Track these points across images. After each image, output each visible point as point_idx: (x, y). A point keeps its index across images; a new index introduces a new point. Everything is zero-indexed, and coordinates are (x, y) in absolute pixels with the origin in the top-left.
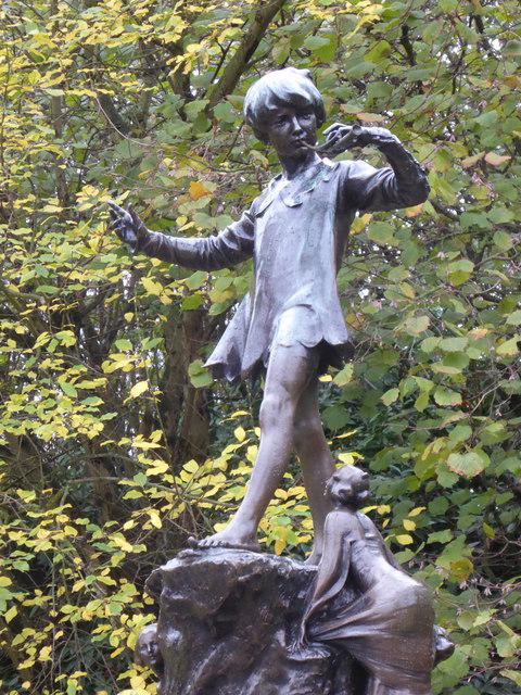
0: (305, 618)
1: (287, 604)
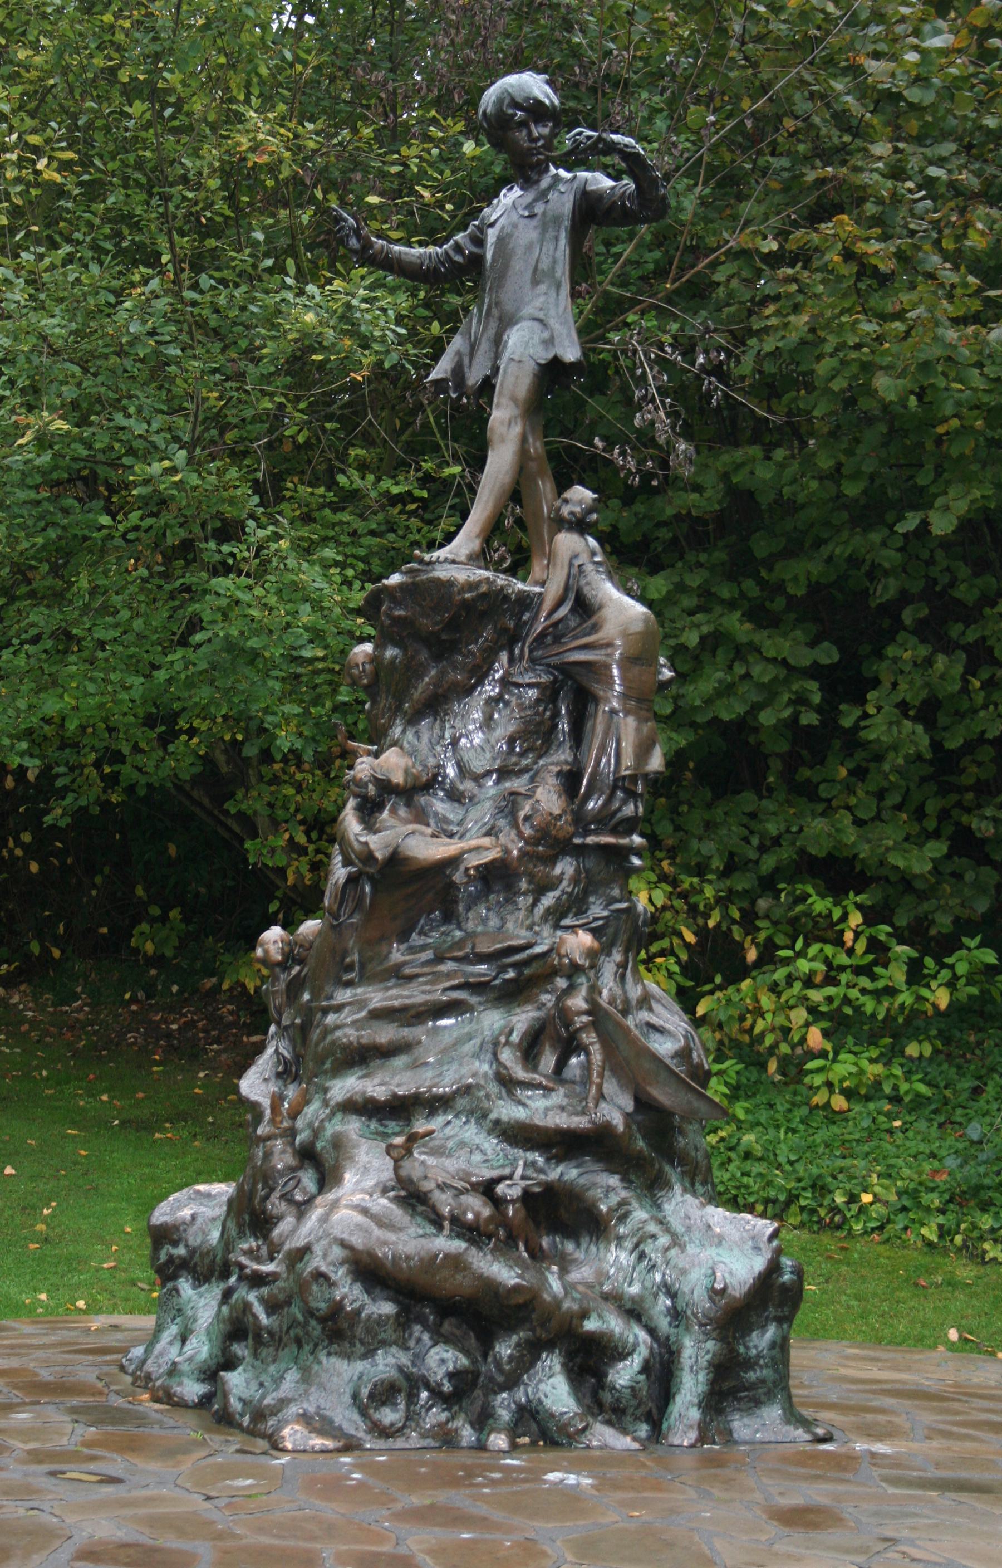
1: (511, 624)
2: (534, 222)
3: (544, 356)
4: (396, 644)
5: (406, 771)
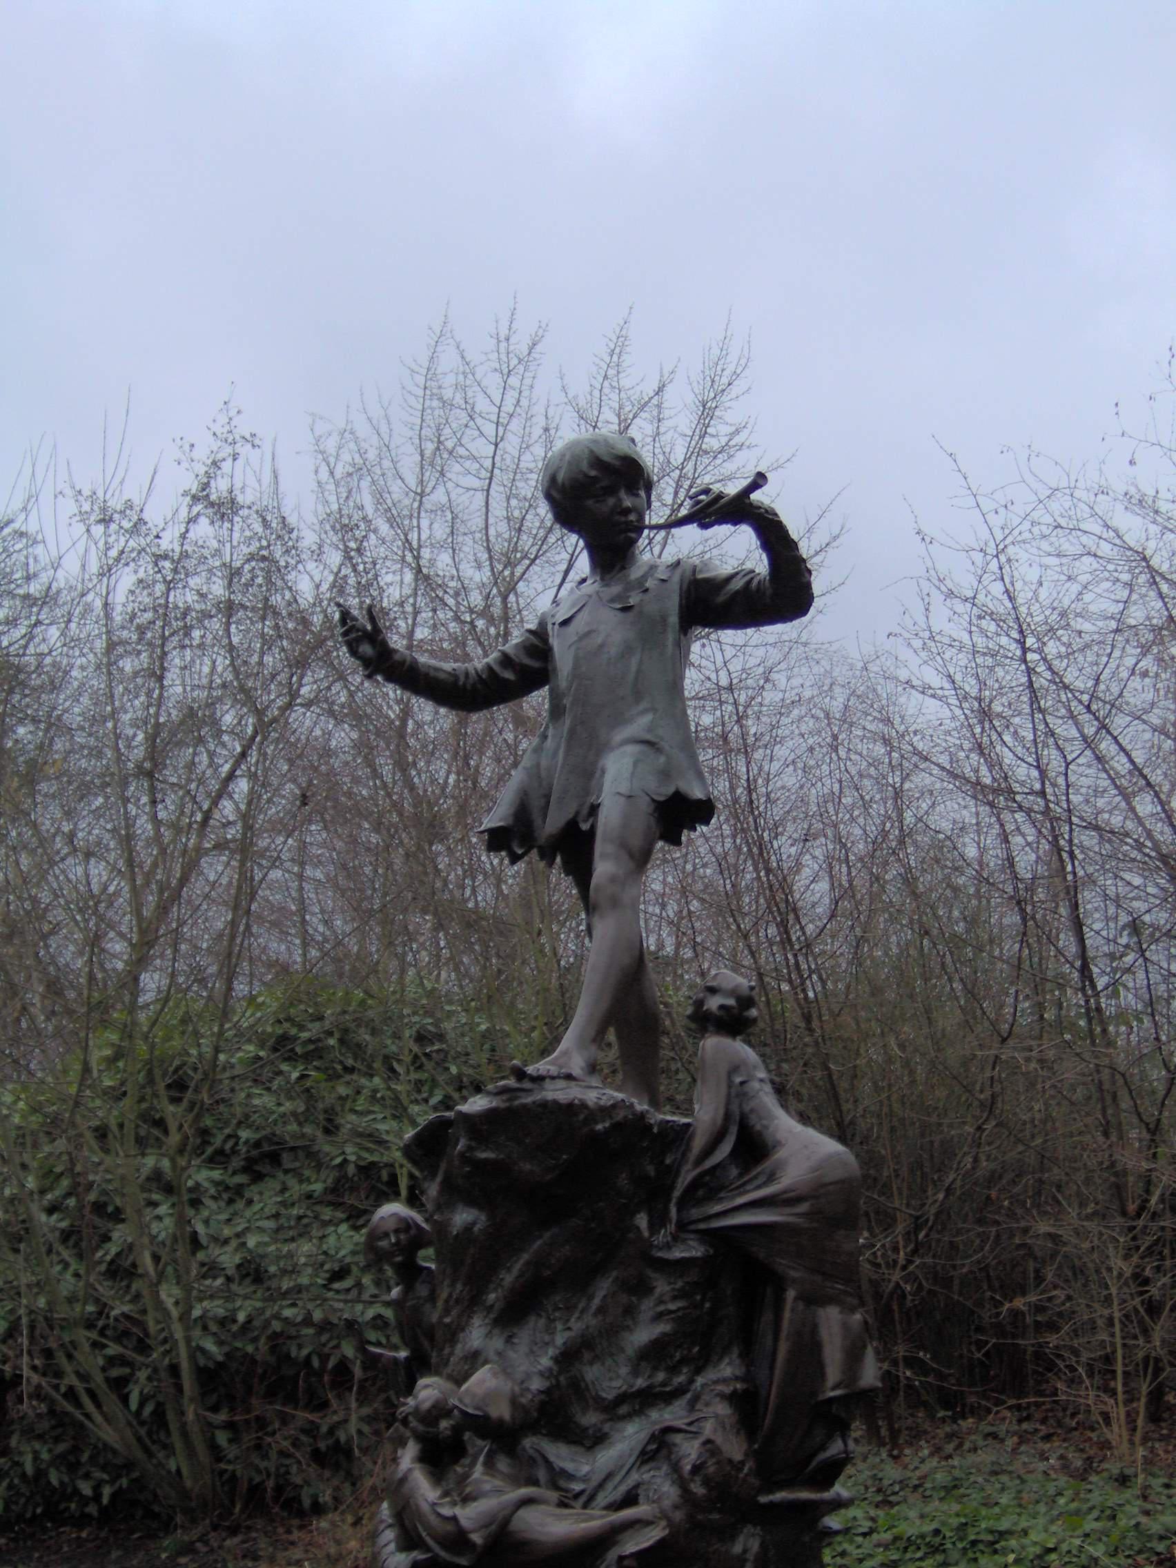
0: (677, 1194)
2: (630, 616)
4: (471, 1202)
5: (514, 1402)
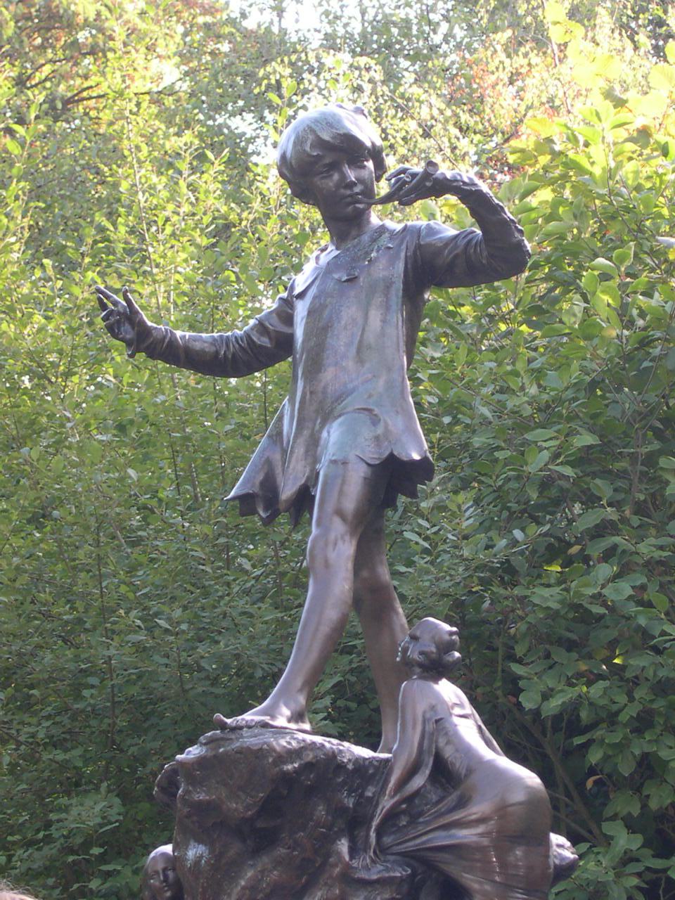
0: (375, 823)
1: (350, 802)
3: (374, 455)
